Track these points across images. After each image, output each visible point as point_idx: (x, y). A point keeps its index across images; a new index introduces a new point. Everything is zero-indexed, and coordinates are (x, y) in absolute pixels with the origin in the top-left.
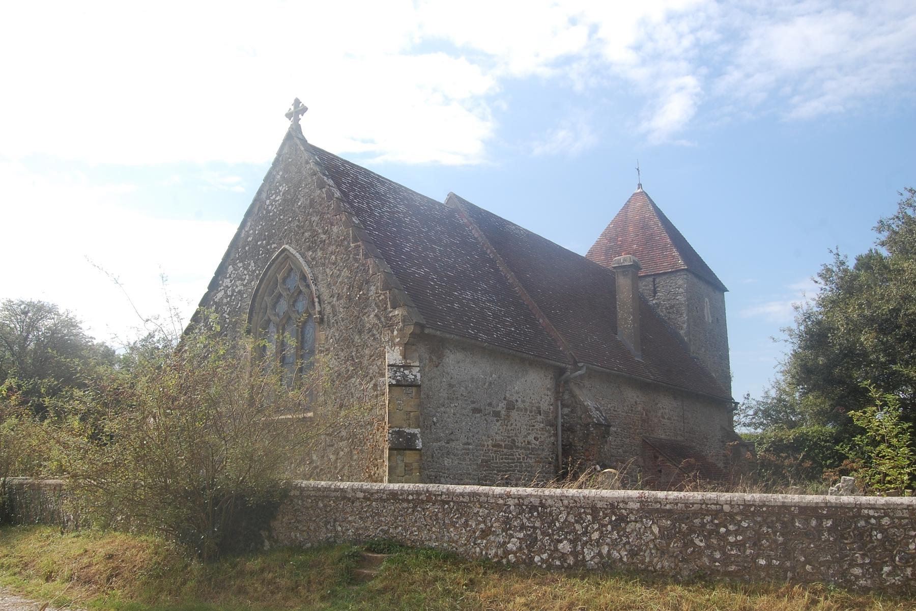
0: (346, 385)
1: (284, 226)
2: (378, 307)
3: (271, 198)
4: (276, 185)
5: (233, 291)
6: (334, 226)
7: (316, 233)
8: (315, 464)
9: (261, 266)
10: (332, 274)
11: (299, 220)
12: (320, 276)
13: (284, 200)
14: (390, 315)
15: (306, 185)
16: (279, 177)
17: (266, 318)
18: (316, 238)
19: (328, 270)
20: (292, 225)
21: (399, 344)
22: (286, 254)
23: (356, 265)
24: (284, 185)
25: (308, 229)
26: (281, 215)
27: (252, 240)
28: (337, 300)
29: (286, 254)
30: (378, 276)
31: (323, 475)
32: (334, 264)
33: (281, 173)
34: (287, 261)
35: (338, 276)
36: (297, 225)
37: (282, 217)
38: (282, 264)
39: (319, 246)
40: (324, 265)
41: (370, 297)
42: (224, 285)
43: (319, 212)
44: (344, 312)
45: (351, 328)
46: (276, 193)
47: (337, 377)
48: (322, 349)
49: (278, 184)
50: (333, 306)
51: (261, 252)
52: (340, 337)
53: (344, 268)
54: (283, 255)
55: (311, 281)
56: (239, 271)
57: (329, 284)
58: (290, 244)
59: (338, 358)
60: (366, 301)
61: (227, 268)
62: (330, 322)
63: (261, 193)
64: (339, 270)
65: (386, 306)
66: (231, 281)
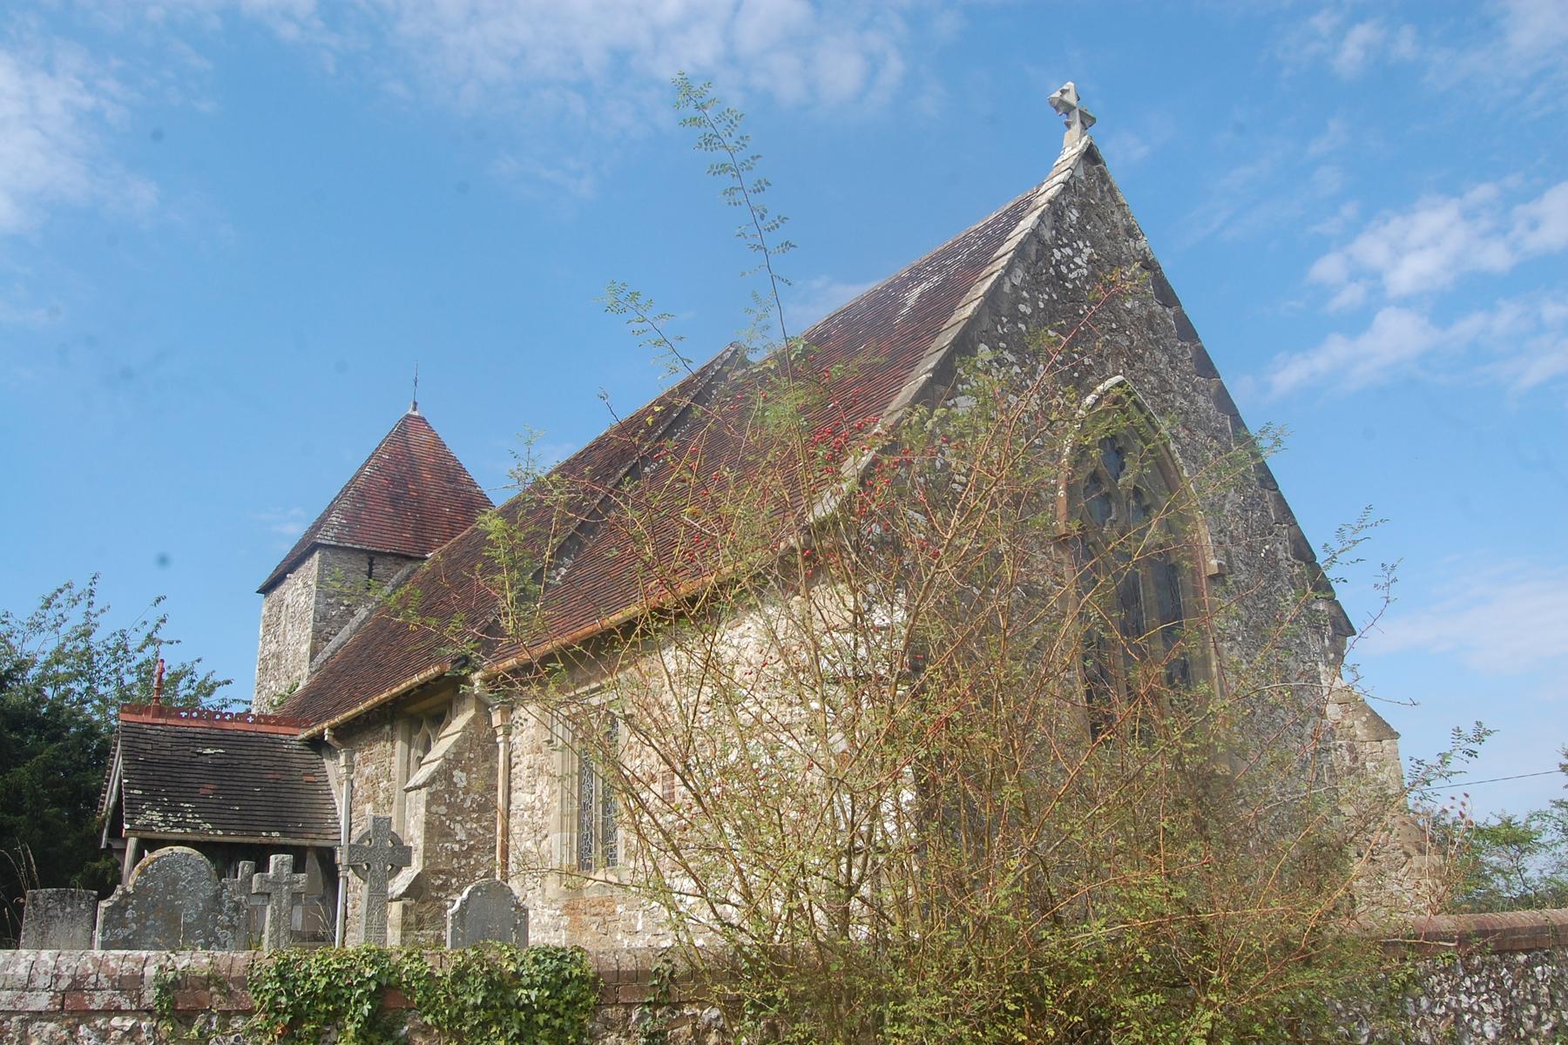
45: (1262, 609)
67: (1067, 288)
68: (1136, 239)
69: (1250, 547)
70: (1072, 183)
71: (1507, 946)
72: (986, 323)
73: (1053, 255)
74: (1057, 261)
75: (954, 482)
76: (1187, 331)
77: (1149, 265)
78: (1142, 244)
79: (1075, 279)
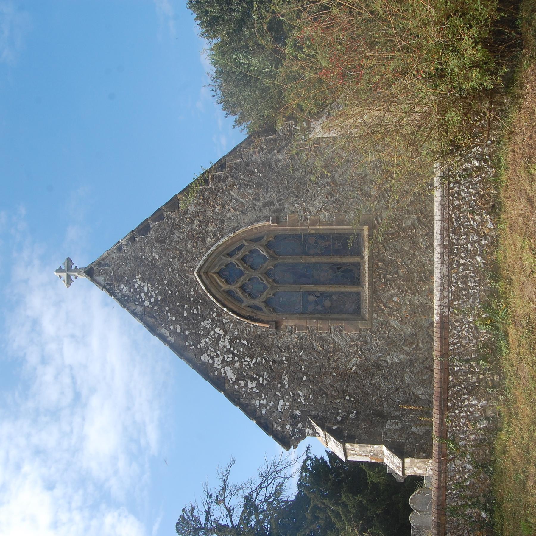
0: (340, 184)
1: (175, 278)
2: (272, 150)
3: (143, 299)
4: (132, 293)
5: (229, 352)
6: (188, 209)
7: (190, 234)
8: (416, 222)
9: (209, 310)
10: (232, 208)
11: (174, 258)
12: (232, 224)
13: (150, 280)
14: (281, 135)
15: (141, 249)
16: (125, 289)
17: (262, 306)
18: (195, 233)
19: (228, 215)
20: (176, 267)
21: (308, 123)
22: (204, 273)
23: (230, 178)
24: (135, 280)
25: (184, 243)
26: (164, 283)
27: (180, 325)
28: (259, 200)
30: (244, 151)
31: (426, 210)
32: (224, 208)
33: (122, 286)
34: (211, 276)
35: (237, 201)
36: (178, 260)
37: (166, 282)
38: (212, 282)
39: (203, 229)
40: (222, 221)
41: (261, 160)
42: (219, 367)
43: (171, 231)
44: (271, 192)
45: (288, 182)
46: (140, 293)
47: (332, 196)
48: (303, 217)
49: (132, 290)
50: (265, 205)
51: (195, 311)
52: (295, 195)
53: (230, 194)
54: (204, 277)
55: (237, 232)
56: (209, 342)
57: (242, 211)
58: (194, 267)
59: (314, 196)
60: (265, 165)
61: (204, 363)
62: (278, 209)
63: (136, 313)
64: (231, 200)
65: (273, 140)
66: (218, 356)
67: (161, 299)
68: (122, 245)
69: (259, 185)
70: (108, 287)
71: (446, 387)
72: (191, 355)
73: (148, 306)
74: (150, 304)
75: (263, 383)
76: (158, 215)
77: (132, 238)
78: (123, 242)
79: (155, 294)
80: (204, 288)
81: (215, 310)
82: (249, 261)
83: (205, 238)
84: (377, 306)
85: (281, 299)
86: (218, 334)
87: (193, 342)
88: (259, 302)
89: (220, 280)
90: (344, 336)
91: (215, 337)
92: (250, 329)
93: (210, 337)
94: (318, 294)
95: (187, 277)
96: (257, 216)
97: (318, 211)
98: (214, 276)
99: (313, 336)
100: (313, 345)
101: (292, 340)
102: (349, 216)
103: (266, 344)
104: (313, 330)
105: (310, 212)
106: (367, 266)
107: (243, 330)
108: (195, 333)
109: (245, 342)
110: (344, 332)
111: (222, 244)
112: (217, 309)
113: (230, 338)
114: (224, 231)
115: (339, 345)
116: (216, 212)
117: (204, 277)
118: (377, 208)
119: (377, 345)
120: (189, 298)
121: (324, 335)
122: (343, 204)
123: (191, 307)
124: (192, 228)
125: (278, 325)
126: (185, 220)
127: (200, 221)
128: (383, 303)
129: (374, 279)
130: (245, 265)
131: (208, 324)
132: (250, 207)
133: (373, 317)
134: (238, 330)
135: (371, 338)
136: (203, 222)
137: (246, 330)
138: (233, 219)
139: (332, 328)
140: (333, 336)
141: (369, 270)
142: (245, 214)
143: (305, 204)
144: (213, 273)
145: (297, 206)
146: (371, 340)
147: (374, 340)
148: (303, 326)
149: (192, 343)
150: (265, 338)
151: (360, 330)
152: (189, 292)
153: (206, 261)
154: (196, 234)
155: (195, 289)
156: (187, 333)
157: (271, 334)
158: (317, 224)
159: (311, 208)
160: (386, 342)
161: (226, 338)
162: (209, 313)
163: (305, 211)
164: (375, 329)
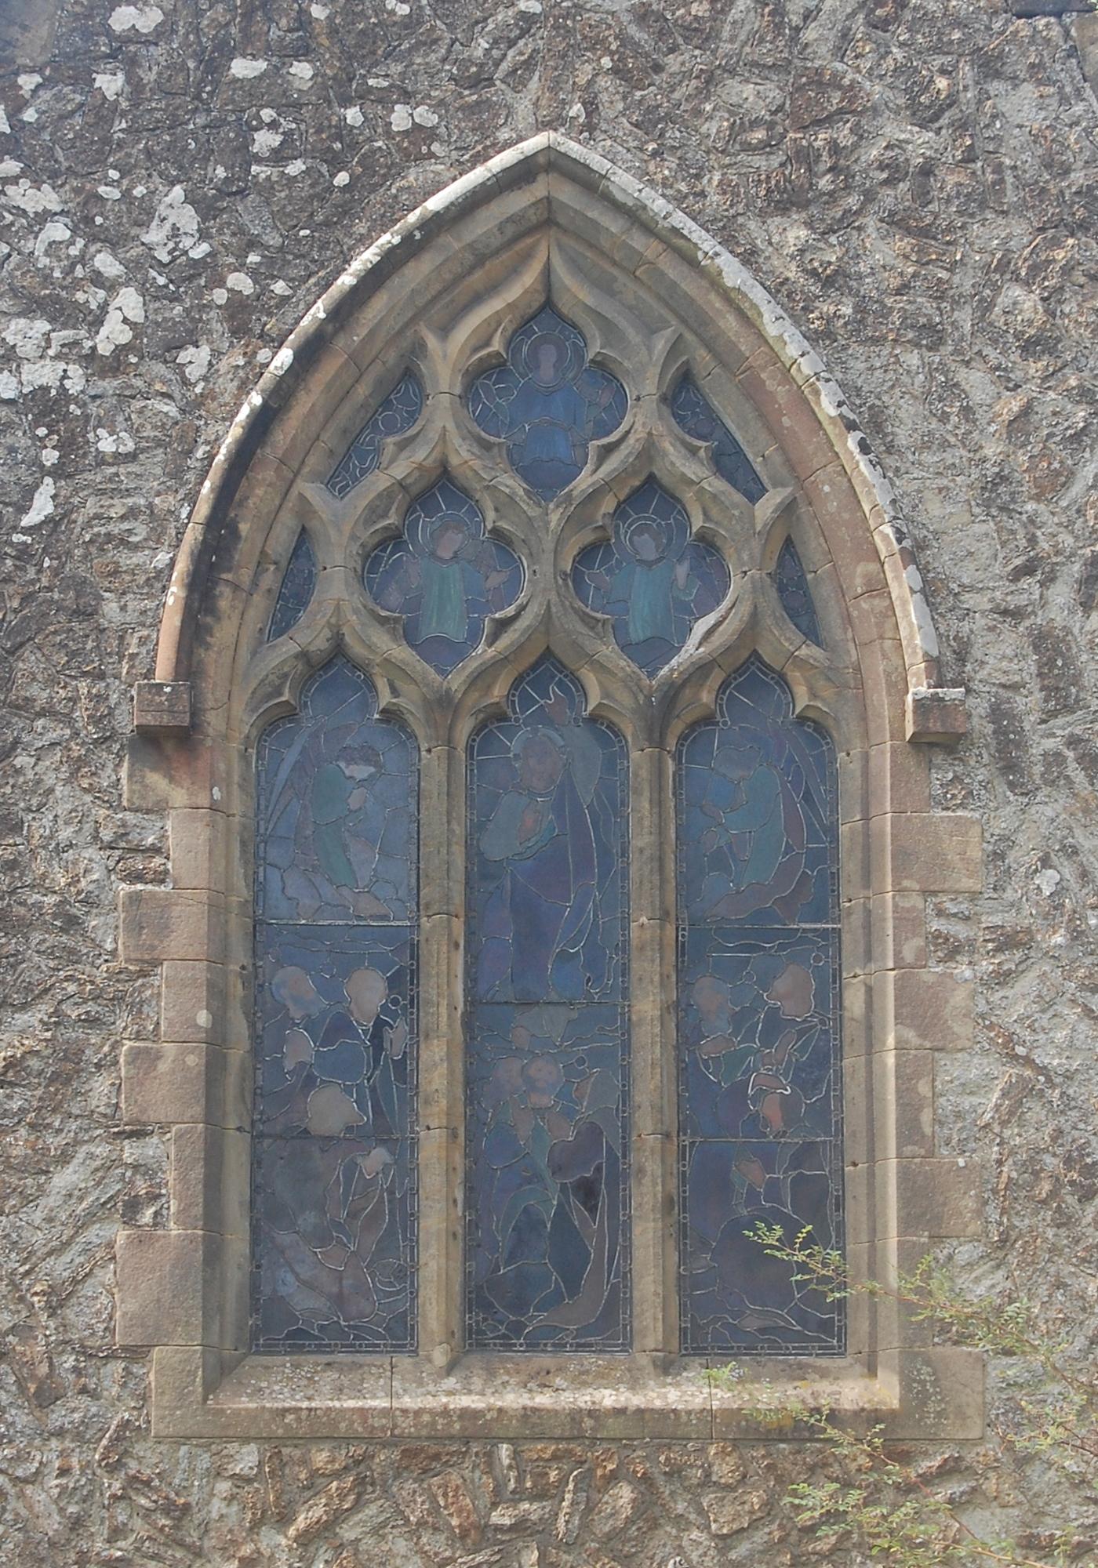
9: (273, 239)
10: (1027, 411)
18: (844, 135)
19: (976, 382)
22: (548, 200)
25: (765, 53)
27: (163, 32)
29: (548, 200)
32: (1030, 347)
34: (527, 256)
38: (480, 260)
39: (869, 196)
40: (932, 335)
48: (961, 931)
51: (265, 141)
54: (518, 201)
55: (852, 442)
56: (38, 246)
57: (1002, 478)
58: (589, 128)
62: (1021, 745)
80: (435, 203)
81: (280, 287)
82: (640, 531)
83: (804, 205)
84: (314, 1474)
85: (361, 771)
86: (104, 307)
87: (40, 128)
88: (338, 607)
89: (493, 324)
90: (94, 1234)
91: (77, 285)
92: (135, 548)
93: (74, 251)
94: (397, 1036)
95: (517, 78)
96: (971, 589)
97: (1010, 1040)
98: (529, 277)
99: (90, 1006)
100: (24, 1007)
101: (59, 850)
102: (970, 1266)
103: (30, 661)
104: (137, 1010)
105: (1003, 978)
106: (608, 1398)
107: (128, 493)
108: (106, 140)
109: (42, 507)
110: (121, 1235)
111: (761, 337)
112: (284, 300)
113: (75, 399)
114: (855, 348)
115: (27, 1200)
116: (997, 289)
117: (518, 201)
118: (1033, 1471)
119: (26, 1481)
120: (364, 96)
121: (100, 1087)
122: (1064, 1220)
123: (297, 106)
124: (875, 111)
125: (169, 747)
126: (938, 61)
127: (927, 170)
128: (337, 1518)
129: (516, 1454)
130: (608, 505)
131: (175, 232)
132: (1032, 540)
133: (232, 1448)
134: (132, 457)
135: (79, 1437)
136: (923, 196)
137: (132, 513)
138: (944, 418)
139: (150, 1149)
140: (91, 1156)
141: (576, 1416)
142: (987, 504)
143: (1059, 939)
144: (547, 271)
145: (1047, 881)
146: (60, 1433)
147: (62, 1454)
148: (164, 929)
149: (29, 115)
150: (72, 655)
151: (135, 1353)
152: (407, 97)
153: (635, 216)
154: (835, 148)
155: (431, 135)
156: (110, 83)
157: (100, 698)
158: (911, 1035)
159: (1028, 983)
160: (52, 1544)
161: (76, 371)
162: (253, 244)
163: (1007, 941)
164: (146, 1458)
